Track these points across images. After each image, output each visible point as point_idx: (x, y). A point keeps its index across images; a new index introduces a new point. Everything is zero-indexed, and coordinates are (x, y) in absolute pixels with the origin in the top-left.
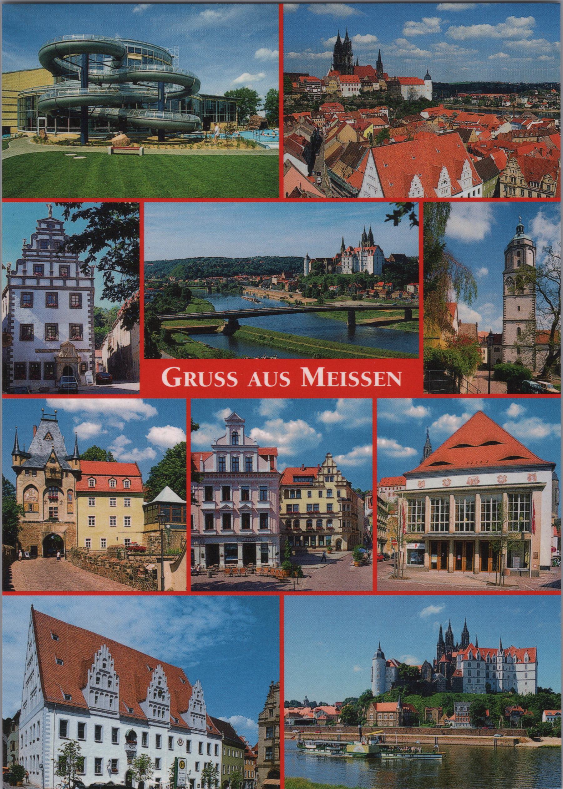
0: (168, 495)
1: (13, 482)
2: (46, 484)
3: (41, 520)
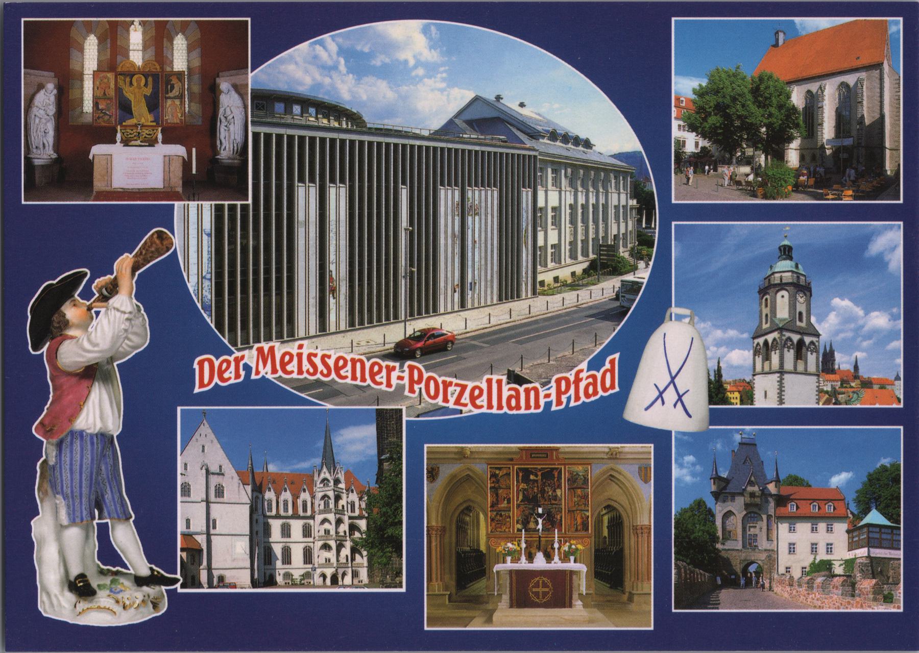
0: (875, 517)
1: (713, 508)
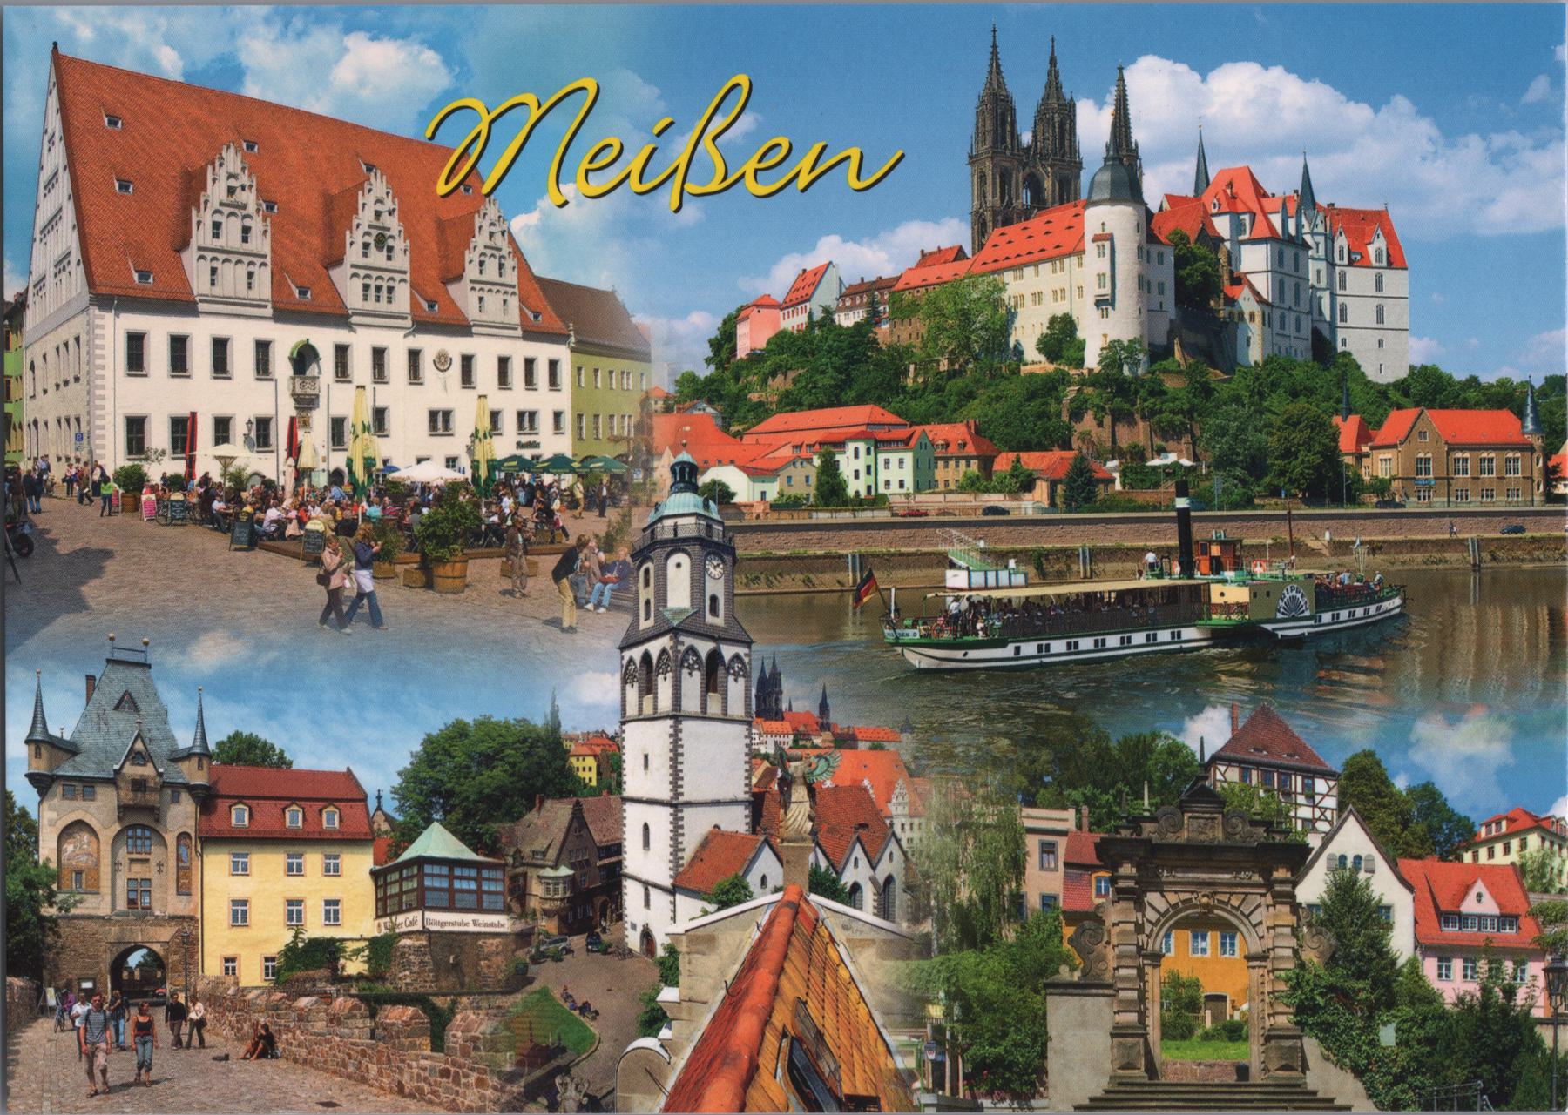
0: (437, 842)
1: (34, 816)
2: (120, 819)
3: (105, 910)
